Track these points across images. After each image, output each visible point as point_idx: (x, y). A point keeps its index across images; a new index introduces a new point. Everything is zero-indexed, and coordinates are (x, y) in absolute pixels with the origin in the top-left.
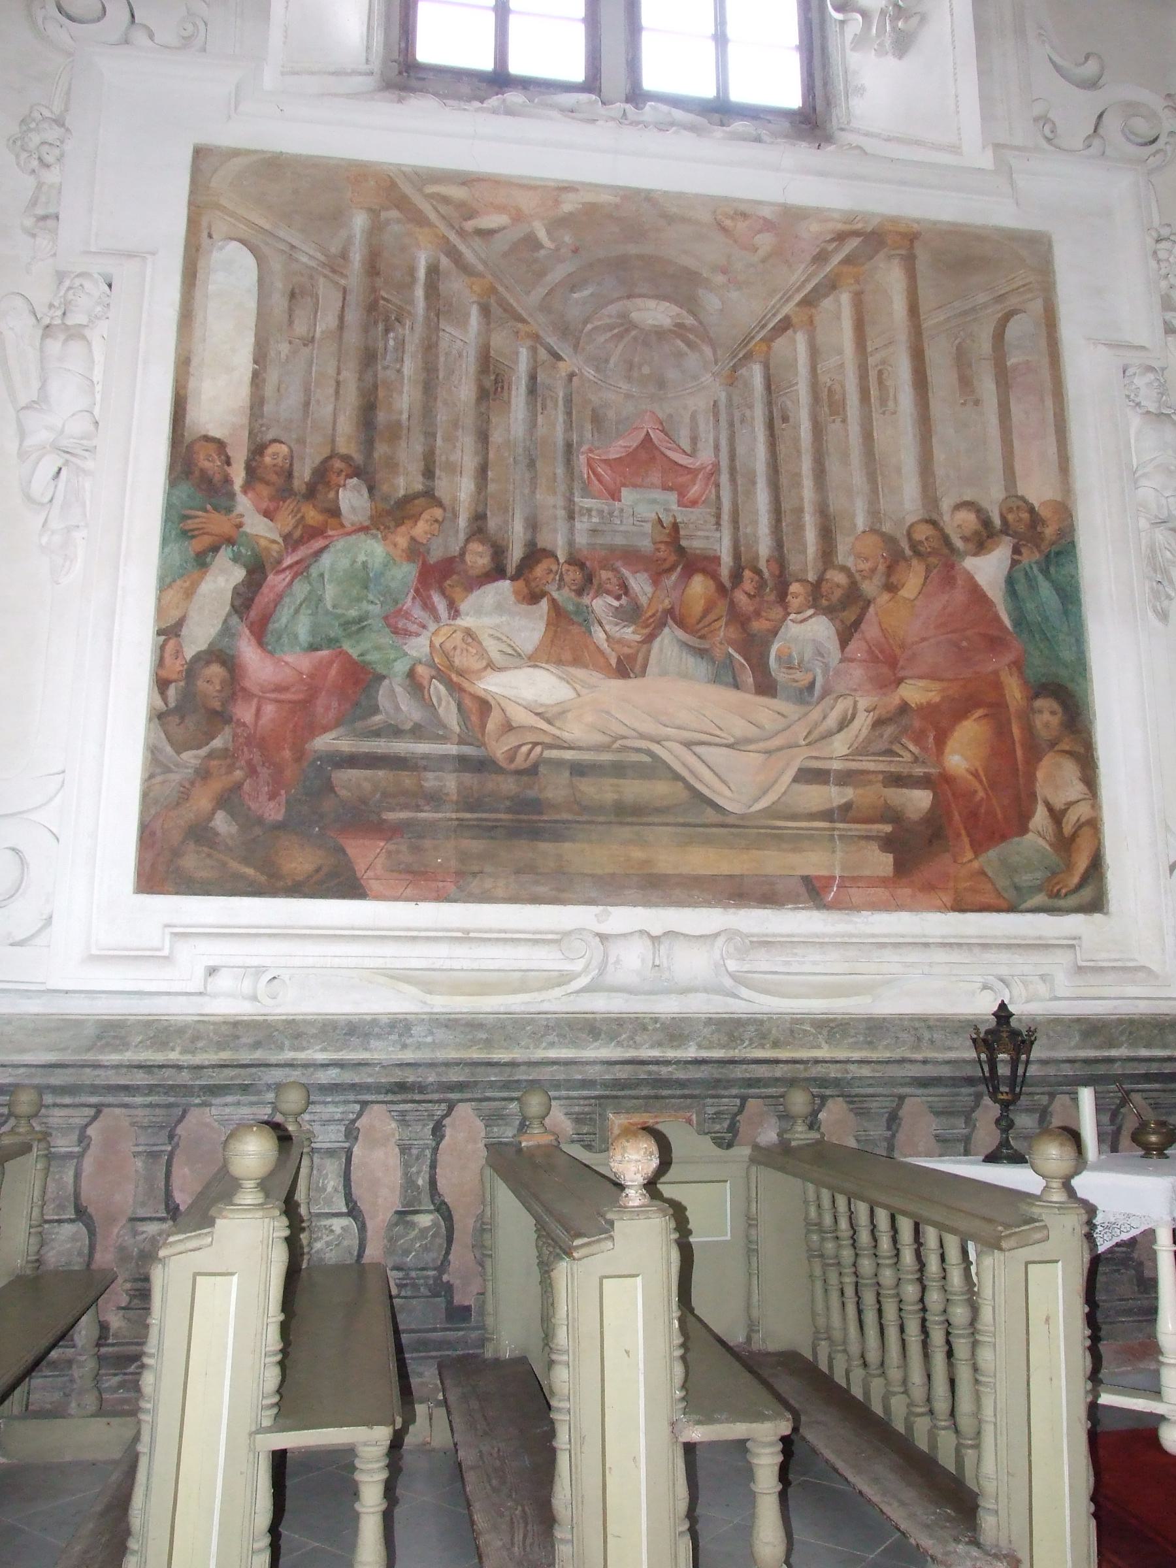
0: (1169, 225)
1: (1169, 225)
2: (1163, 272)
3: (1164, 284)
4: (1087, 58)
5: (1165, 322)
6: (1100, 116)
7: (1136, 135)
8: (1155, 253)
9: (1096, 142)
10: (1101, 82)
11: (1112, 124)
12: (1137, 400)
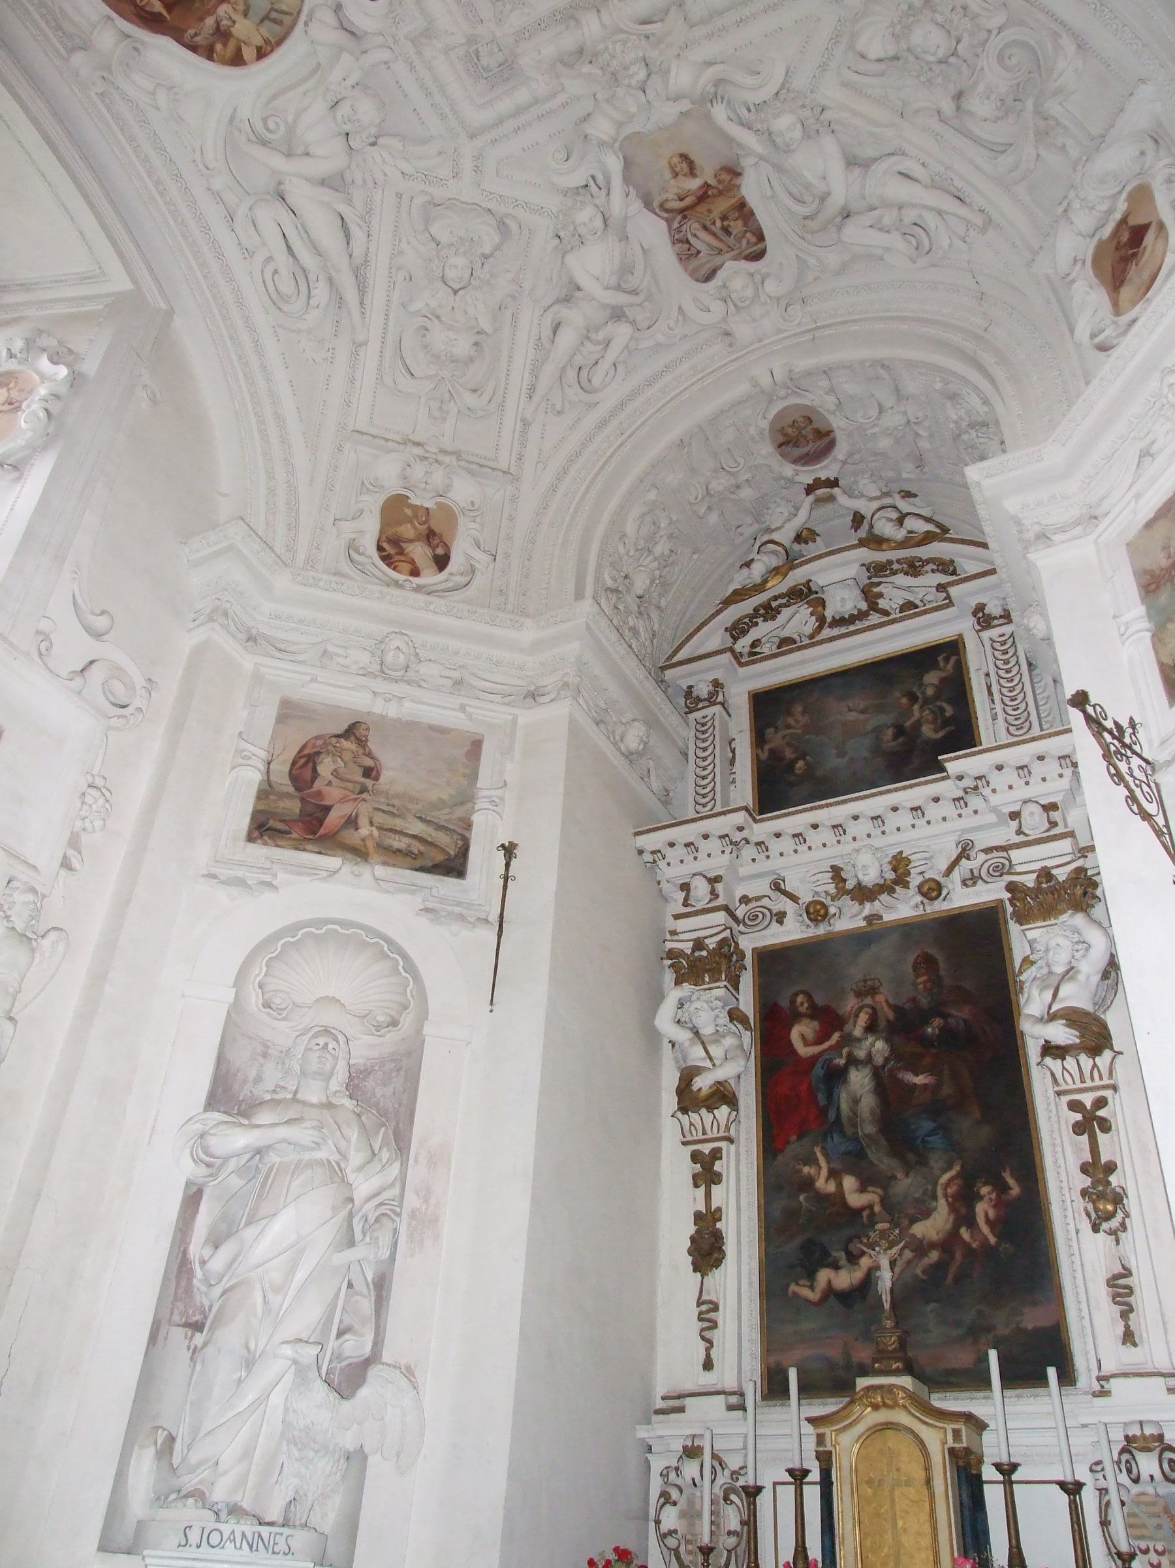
0: (105, 778)
1: (105, 778)
2: (83, 813)
3: (79, 824)
4: (103, 613)
5: (65, 857)
6: (92, 662)
7: (112, 694)
8: (84, 794)
9: (78, 681)
10: (105, 638)
11: (97, 674)
12: (9, 913)
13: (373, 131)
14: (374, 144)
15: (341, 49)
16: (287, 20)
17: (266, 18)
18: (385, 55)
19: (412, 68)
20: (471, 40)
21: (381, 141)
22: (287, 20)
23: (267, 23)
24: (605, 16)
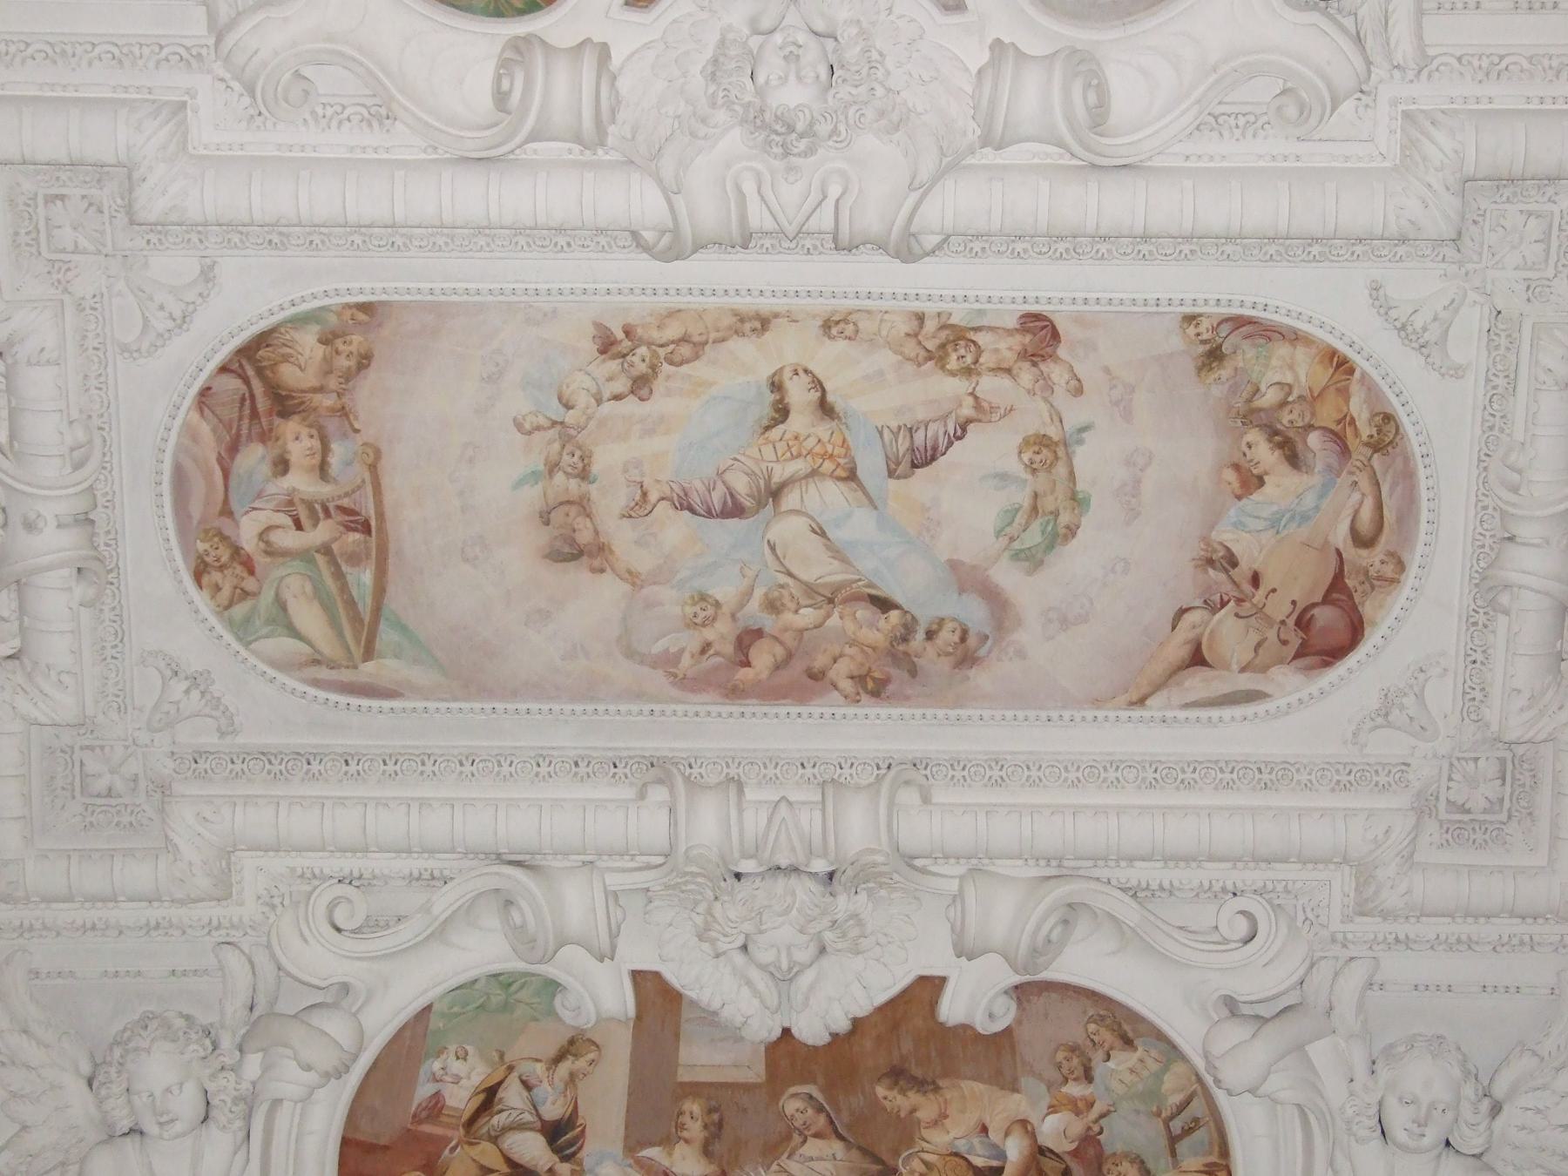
13: (1469, 1091)
14: (1496, 1109)
15: (1299, 1048)
16: (1197, 1108)
17: (1173, 1140)
18: (1354, 978)
19: (1406, 943)
20: (1423, 808)
21: (1499, 1090)
22: (1197, 1108)
23: (1183, 1147)
24: (1525, 531)
